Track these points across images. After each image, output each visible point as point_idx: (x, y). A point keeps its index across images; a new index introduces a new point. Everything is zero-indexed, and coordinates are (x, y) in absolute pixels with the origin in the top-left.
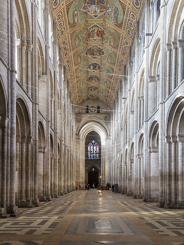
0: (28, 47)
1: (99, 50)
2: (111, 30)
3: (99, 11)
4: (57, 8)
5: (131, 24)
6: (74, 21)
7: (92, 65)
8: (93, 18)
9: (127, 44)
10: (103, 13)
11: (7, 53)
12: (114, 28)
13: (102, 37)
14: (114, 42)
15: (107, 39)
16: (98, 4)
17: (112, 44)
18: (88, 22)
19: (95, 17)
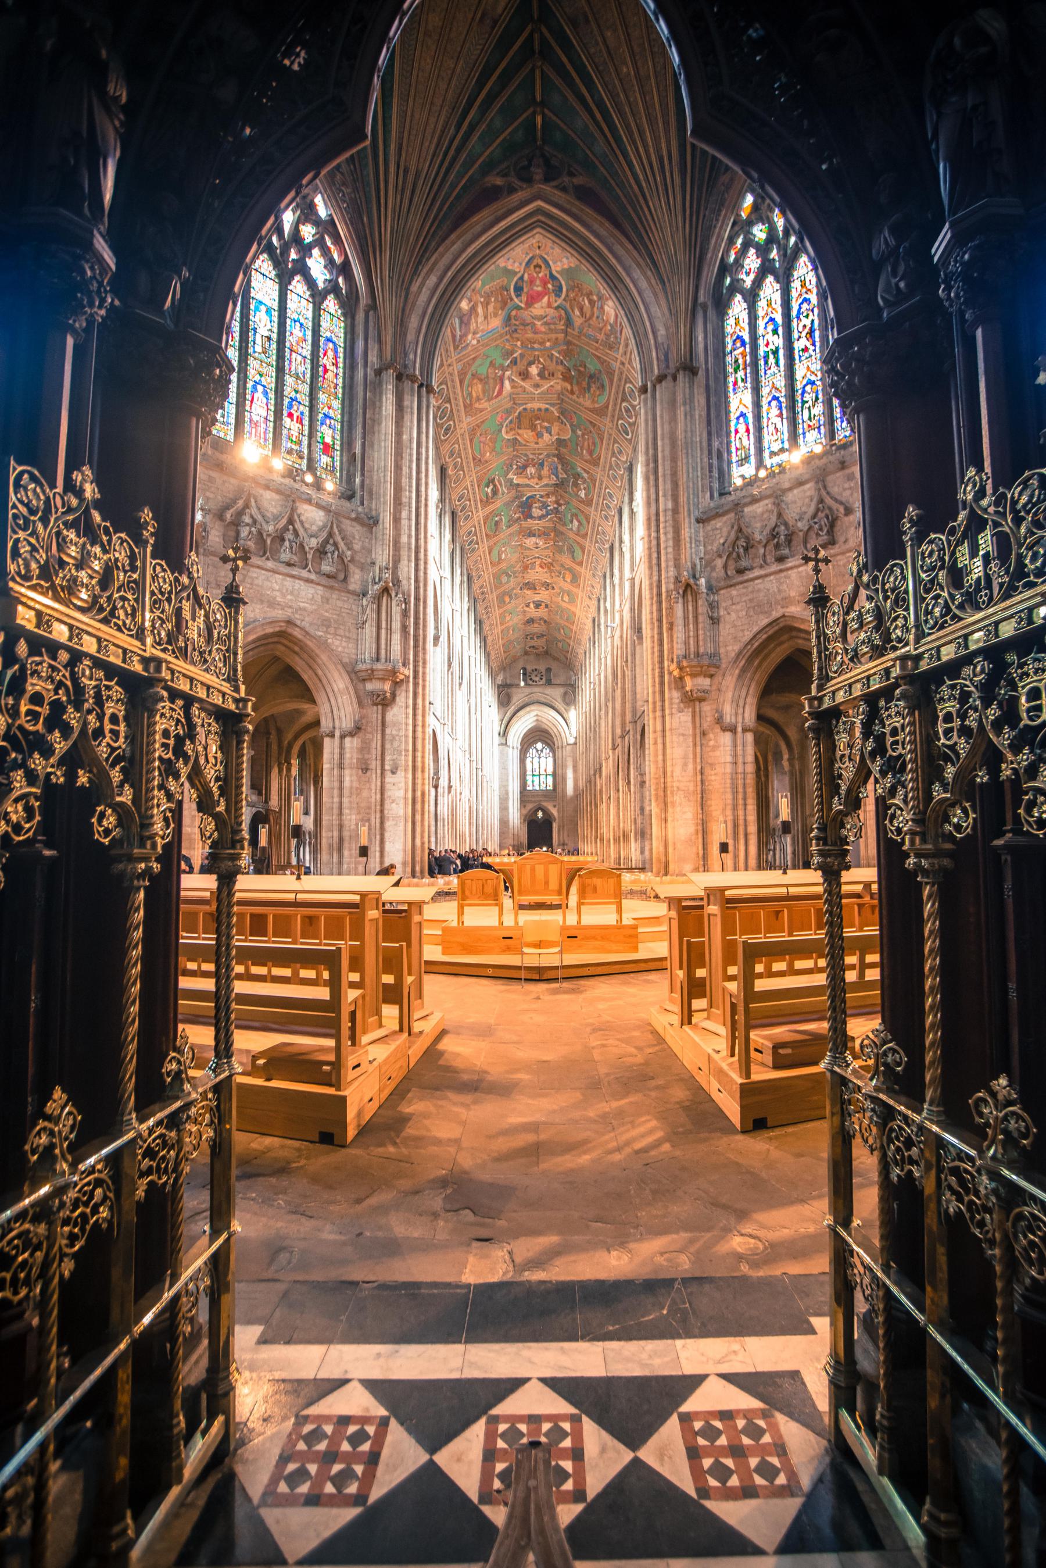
6: (500, 559)
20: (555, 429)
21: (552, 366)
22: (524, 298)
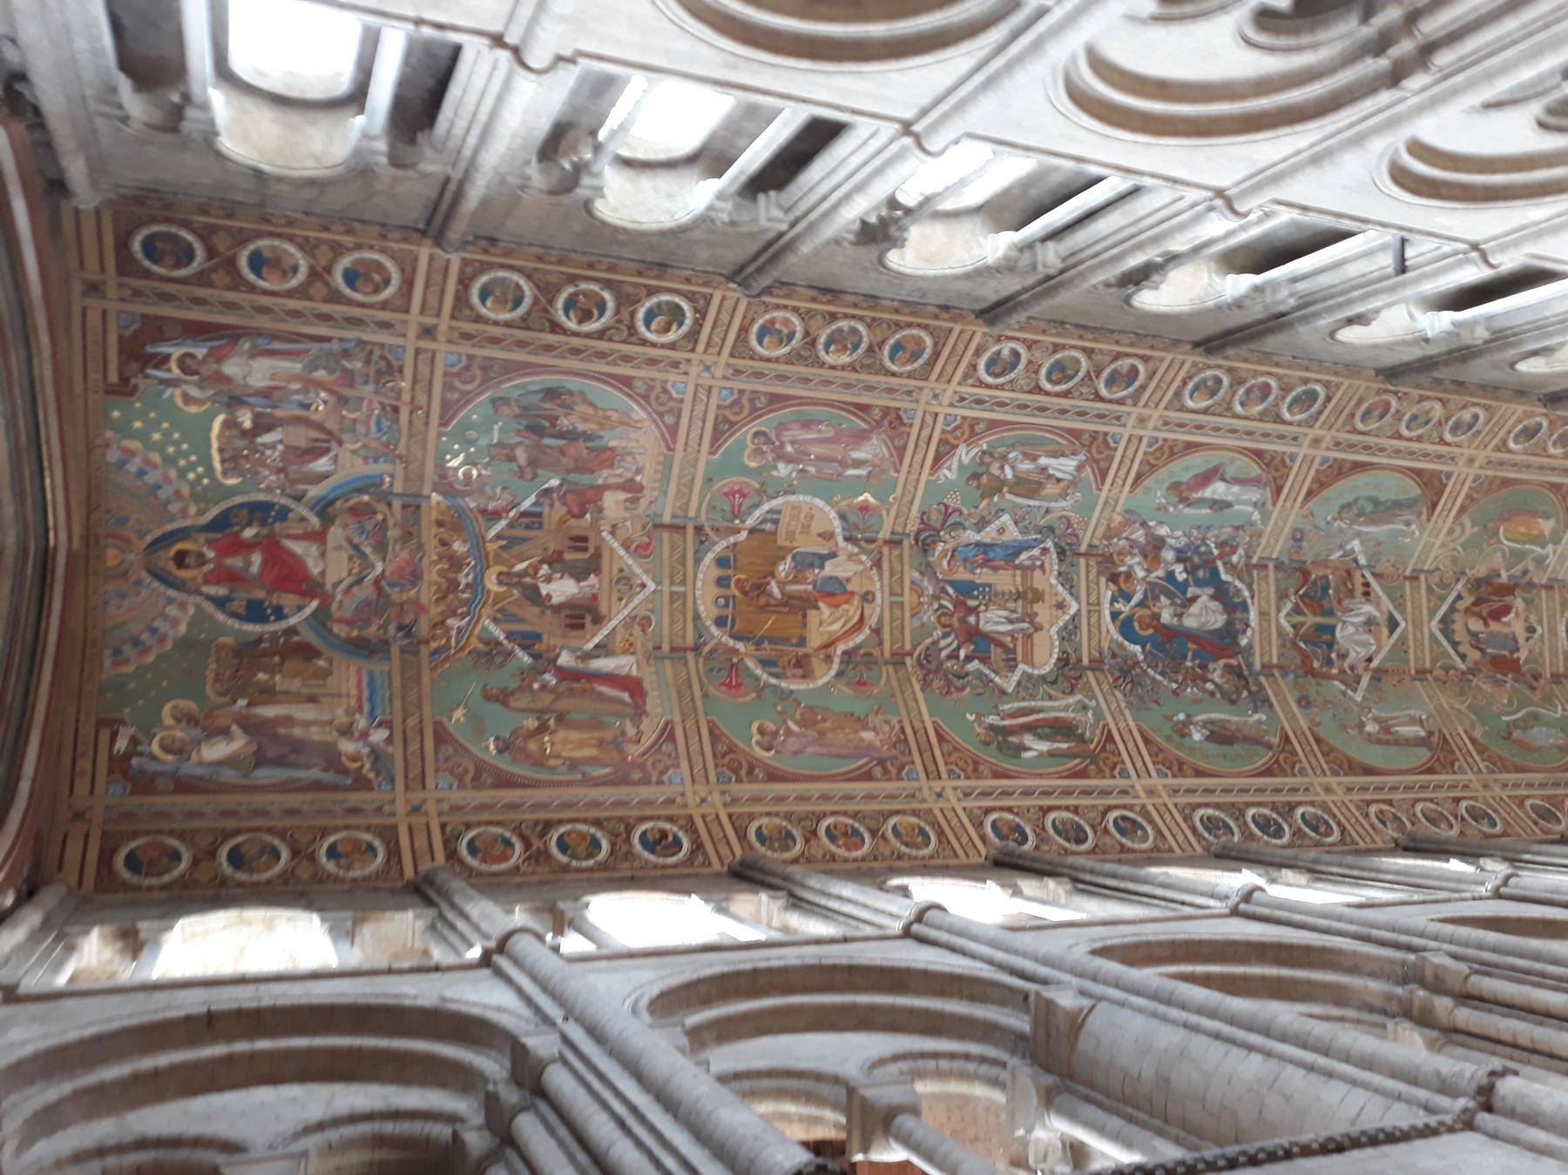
0: (1437, 985)
2: (1463, 539)
3: (1368, 609)
4: (1339, 823)
5: (1414, 418)
9: (1530, 433)
11: (1358, 1097)
12: (1451, 519)
13: (1509, 590)
14: (1535, 513)
15: (1518, 556)
16: (1330, 613)
17: (1547, 526)
18: (1428, 665)
19: (1399, 631)
22: (288, 600)
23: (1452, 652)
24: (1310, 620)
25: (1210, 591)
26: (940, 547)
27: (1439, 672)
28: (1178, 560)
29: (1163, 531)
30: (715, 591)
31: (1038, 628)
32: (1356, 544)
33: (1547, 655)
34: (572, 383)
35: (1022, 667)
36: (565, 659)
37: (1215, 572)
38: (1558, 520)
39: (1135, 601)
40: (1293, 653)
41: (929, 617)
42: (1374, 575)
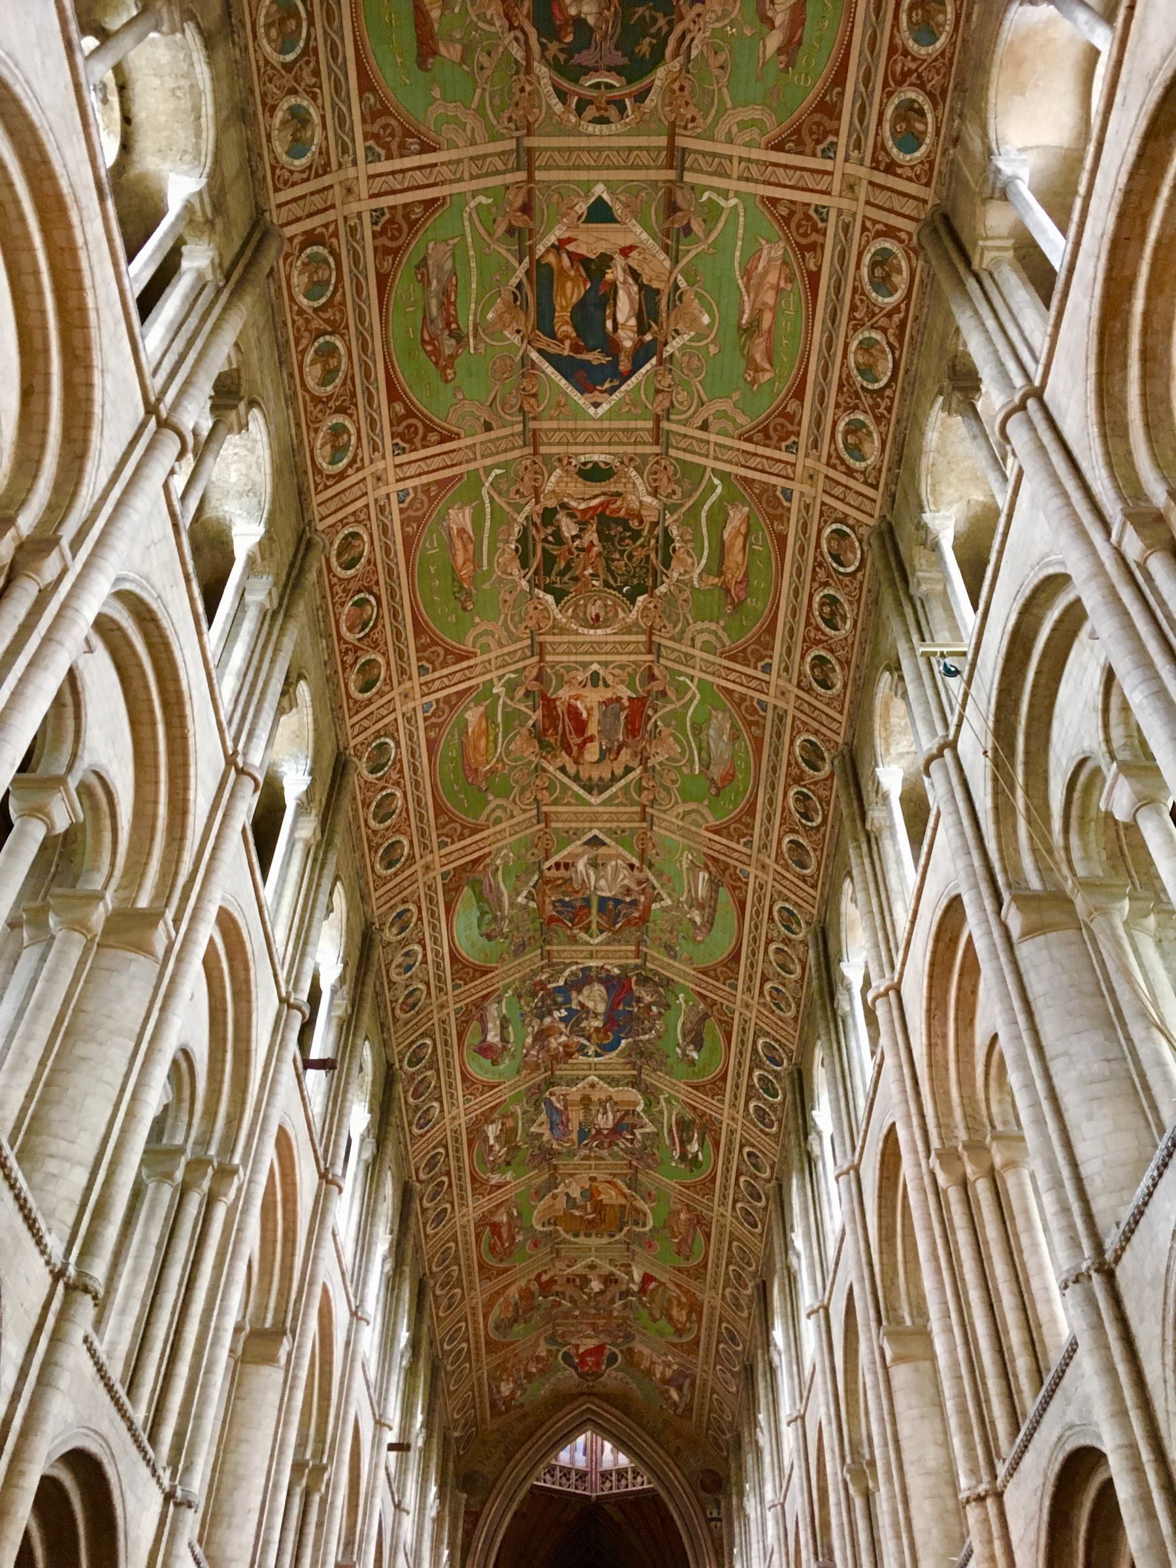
1: (562, 574)
3: (581, 865)
7: (625, 365)
8: (611, 833)
10: (556, 858)
13: (549, 704)
16: (587, 901)
18: (638, 809)
19: (601, 836)
20: (561, 1203)
21: (570, 1290)
22: (607, 1352)
23: (623, 782)
24: (594, 917)
25: (574, 994)
26: (555, 1146)
27: (645, 797)
28: (550, 1014)
29: (529, 1040)
30: (593, 1238)
31: (610, 1098)
32: (520, 900)
33: (625, 658)
34: (491, 1324)
35: (639, 1109)
36: (635, 1288)
37: (557, 990)
38: (467, 709)
39: (585, 1042)
40: (626, 933)
41: (605, 1153)
42: (547, 859)
